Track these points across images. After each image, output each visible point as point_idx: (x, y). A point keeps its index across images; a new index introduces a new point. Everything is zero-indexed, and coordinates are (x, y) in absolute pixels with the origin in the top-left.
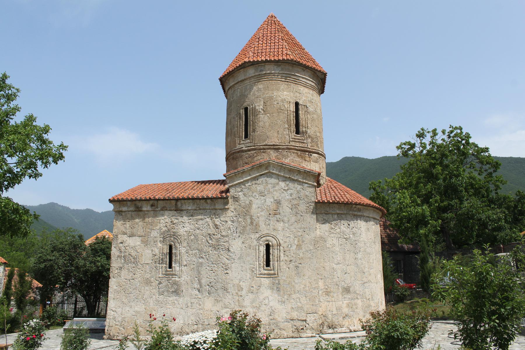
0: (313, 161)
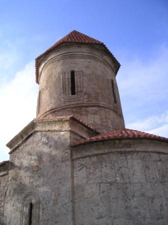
0: (91, 114)
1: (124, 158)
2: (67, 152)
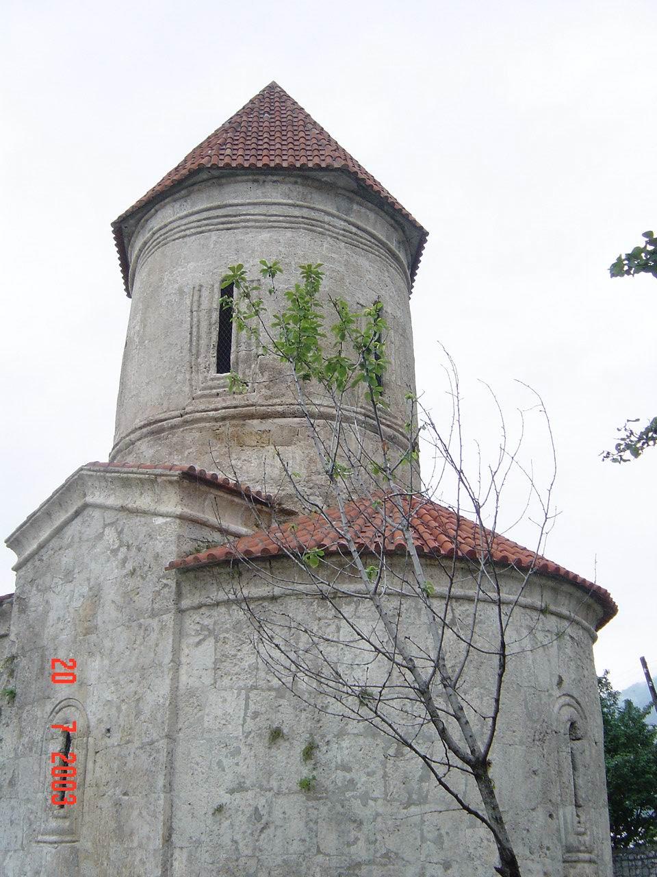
2: (166, 585)
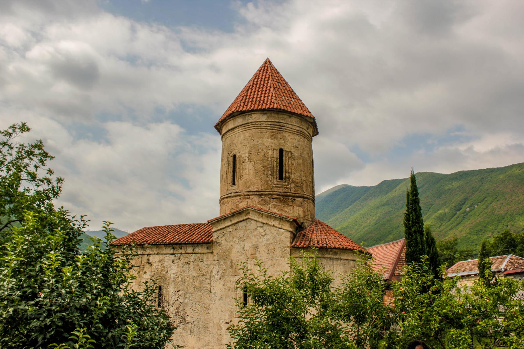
0: (296, 206)
1: (331, 263)
